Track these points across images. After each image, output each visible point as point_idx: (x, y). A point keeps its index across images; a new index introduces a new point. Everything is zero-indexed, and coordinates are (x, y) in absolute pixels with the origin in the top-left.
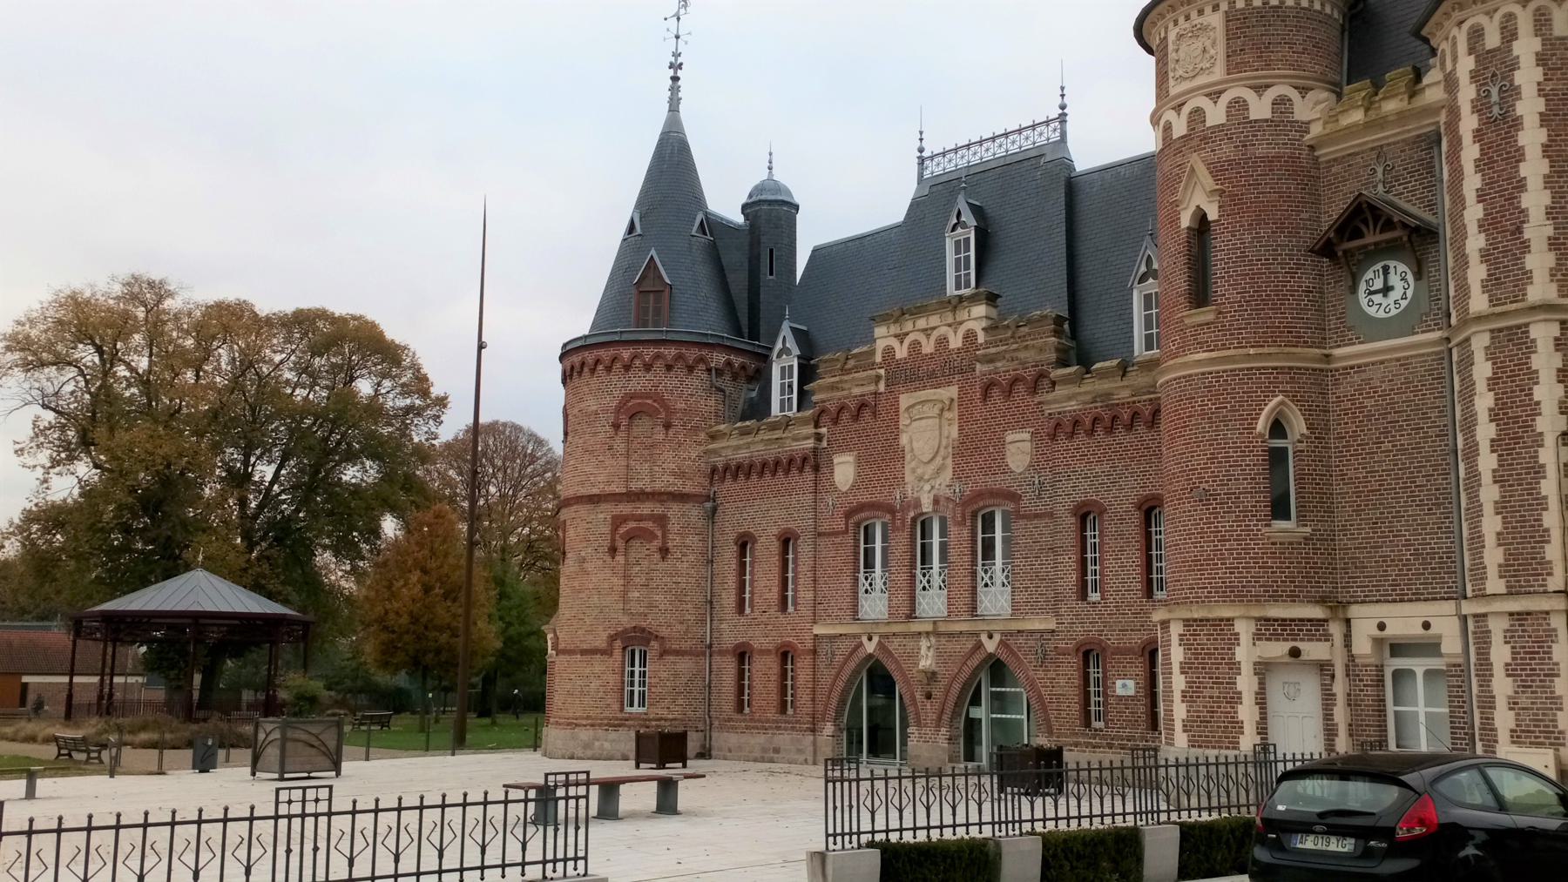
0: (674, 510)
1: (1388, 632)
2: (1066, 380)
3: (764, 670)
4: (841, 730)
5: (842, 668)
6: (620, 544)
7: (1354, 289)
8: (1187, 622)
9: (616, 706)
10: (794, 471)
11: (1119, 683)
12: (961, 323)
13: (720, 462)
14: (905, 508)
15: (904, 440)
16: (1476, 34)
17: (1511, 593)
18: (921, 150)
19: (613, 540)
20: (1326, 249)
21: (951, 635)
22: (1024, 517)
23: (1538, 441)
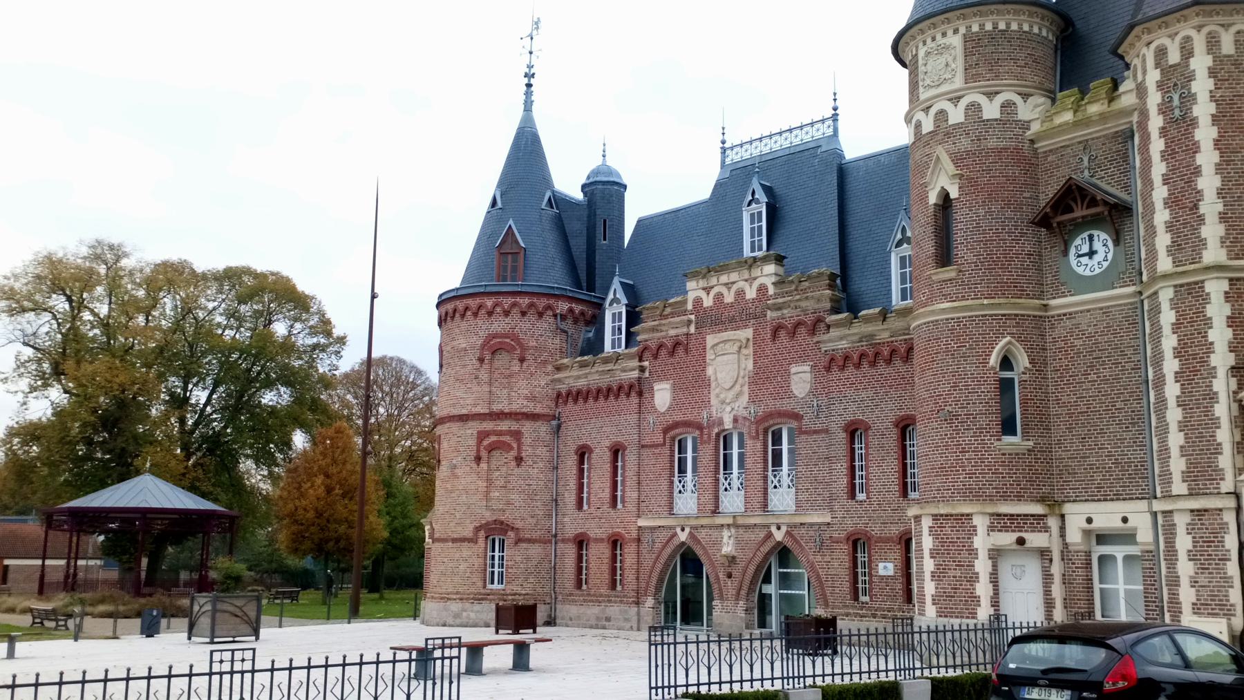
0: (527, 427)
1: (1094, 525)
2: (838, 324)
3: (598, 555)
4: (659, 603)
5: (660, 552)
6: (484, 454)
7: (1066, 253)
8: (936, 517)
9: (480, 584)
10: (623, 396)
11: (881, 565)
12: (755, 279)
13: (563, 388)
14: (711, 425)
15: (710, 371)
16: (1161, 53)
17: (1192, 494)
18: (723, 142)
19: (478, 451)
20: (1043, 221)
21: (747, 527)
22: (805, 433)
23: (1212, 372)
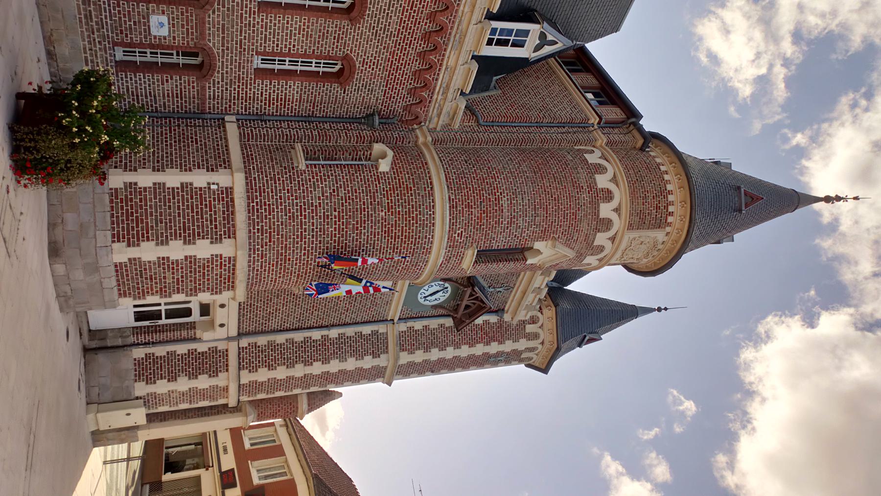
1: (219, 310)
11: (164, 19)
